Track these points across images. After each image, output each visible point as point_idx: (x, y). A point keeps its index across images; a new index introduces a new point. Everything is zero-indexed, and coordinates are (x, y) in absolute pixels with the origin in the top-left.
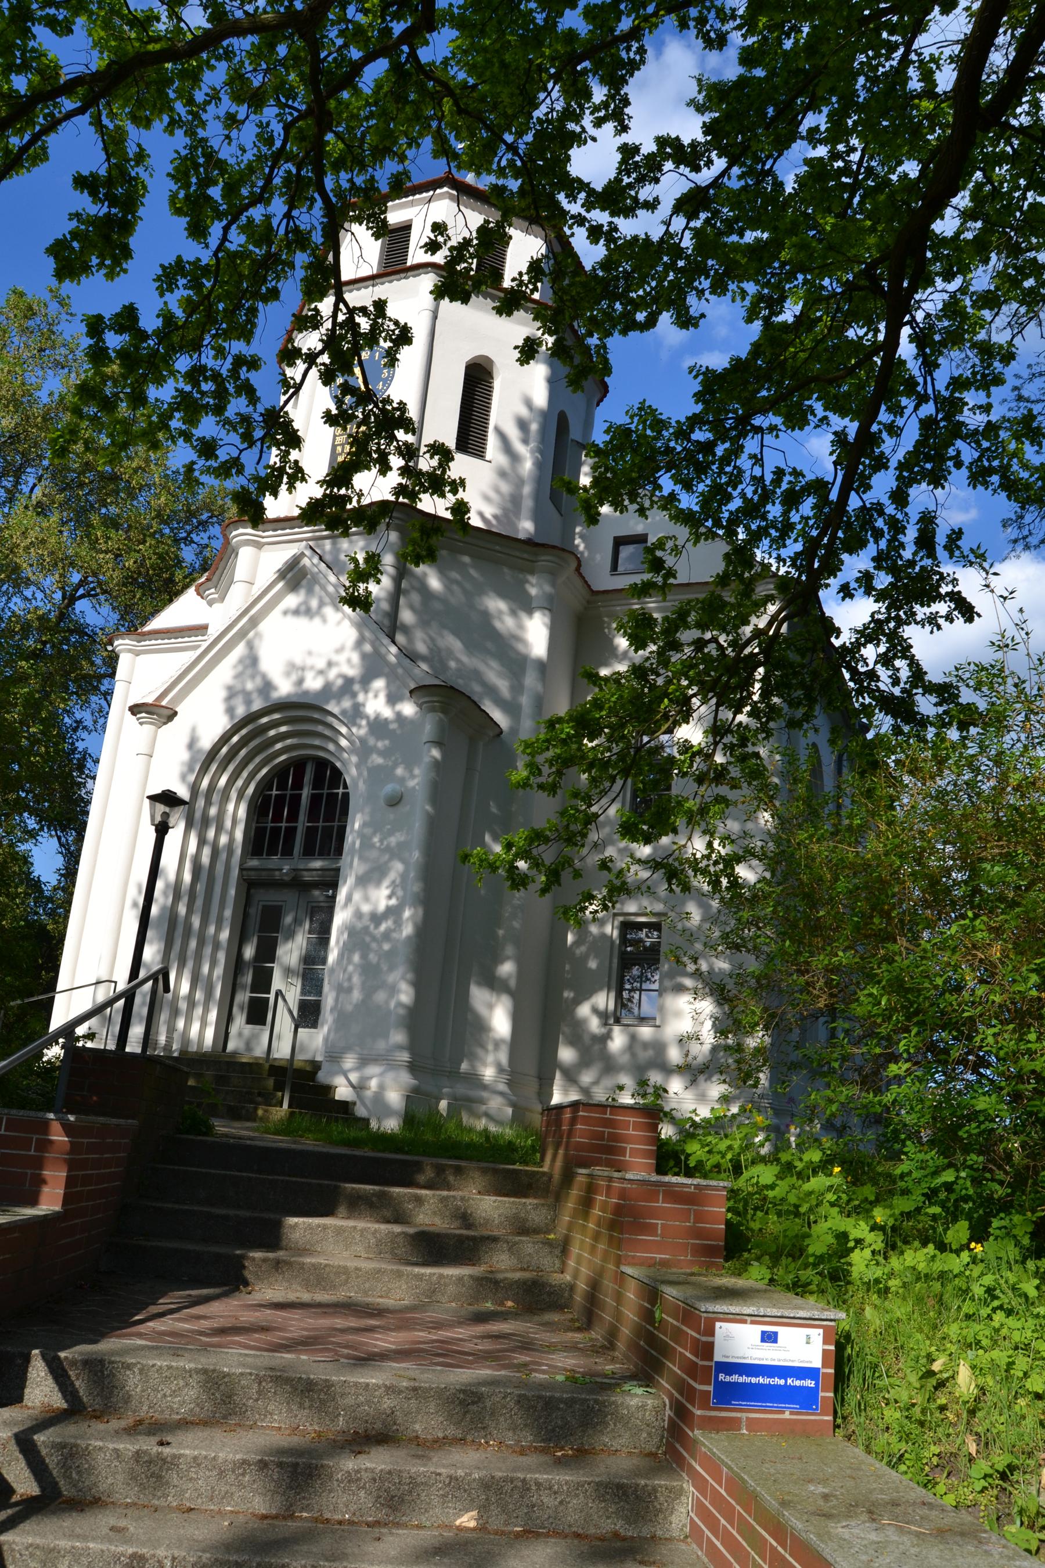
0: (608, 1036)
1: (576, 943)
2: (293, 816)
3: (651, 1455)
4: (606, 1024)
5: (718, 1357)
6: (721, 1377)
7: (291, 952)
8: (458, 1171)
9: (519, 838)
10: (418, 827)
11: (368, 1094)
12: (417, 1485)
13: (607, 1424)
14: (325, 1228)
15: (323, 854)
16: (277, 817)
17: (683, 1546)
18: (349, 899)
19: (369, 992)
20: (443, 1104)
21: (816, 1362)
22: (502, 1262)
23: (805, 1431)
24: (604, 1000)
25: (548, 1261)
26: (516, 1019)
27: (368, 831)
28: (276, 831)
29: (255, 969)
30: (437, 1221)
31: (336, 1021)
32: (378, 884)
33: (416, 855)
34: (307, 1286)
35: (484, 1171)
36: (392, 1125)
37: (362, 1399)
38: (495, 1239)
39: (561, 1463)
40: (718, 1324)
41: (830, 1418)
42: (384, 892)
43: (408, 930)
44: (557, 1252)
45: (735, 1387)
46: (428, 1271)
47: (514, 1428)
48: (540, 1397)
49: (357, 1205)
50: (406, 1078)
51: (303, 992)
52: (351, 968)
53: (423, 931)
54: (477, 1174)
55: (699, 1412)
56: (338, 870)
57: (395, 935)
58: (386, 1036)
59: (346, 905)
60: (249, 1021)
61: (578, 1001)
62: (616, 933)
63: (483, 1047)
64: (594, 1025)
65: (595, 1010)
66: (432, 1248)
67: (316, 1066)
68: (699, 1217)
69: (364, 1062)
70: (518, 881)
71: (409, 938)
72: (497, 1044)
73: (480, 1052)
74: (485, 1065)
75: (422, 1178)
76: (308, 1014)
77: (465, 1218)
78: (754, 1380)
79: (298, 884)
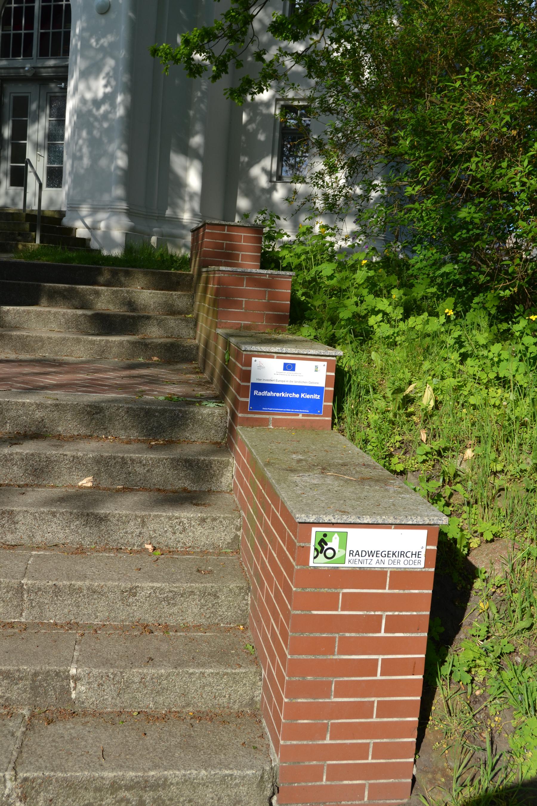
0: (273, 188)
1: (249, 122)
2: (30, 25)
3: (217, 443)
4: (270, 181)
5: (253, 380)
6: (256, 393)
7: (37, 131)
8: (127, 274)
9: (194, 35)
10: (123, 28)
11: (99, 232)
12: (51, 462)
13: (188, 426)
14: (29, 312)
15: (55, 54)
16: (17, 26)
17: (227, 495)
18: (76, 89)
19: (95, 159)
20: (154, 239)
21: (322, 383)
22: (154, 333)
23: (312, 427)
24: (269, 163)
25: (185, 331)
26: (205, 177)
27: (86, 34)
28: (17, 37)
29: (13, 144)
30: (111, 307)
31: (73, 181)
32: (97, 77)
33: (122, 53)
34: (15, 350)
35: (146, 274)
36: (117, 252)
37: (21, 412)
38: (148, 318)
39: (151, 448)
40: (254, 359)
41: (330, 419)
42: (102, 82)
43: (120, 112)
44: (191, 325)
45: (265, 398)
46: (99, 338)
47: (125, 428)
48: (142, 409)
49: (54, 297)
50: (125, 221)
51: (50, 161)
52: (81, 142)
53: (132, 112)
54: (141, 276)
55: (240, 415)
56: (67, 67)
57: (111, 116)
58: (109, 191)
59: (74, 93)
60: (13, 184)
61: (251, 164)
62: (278, 112)
63: (182, 198)
64: (263, 181)
65: (264, 170)
66: (105, 324)
67: (62, 214)
68: (273, 296)
69: (95, 210)
70: (196, 70)
71: (121, 118)
72: (192, 196)
73: (180, 202)
74: (183, 211)
75: (101, 279)
76: (55, 177)
77: (131, 304)
78: (278, 395)
79: (37, 79)
